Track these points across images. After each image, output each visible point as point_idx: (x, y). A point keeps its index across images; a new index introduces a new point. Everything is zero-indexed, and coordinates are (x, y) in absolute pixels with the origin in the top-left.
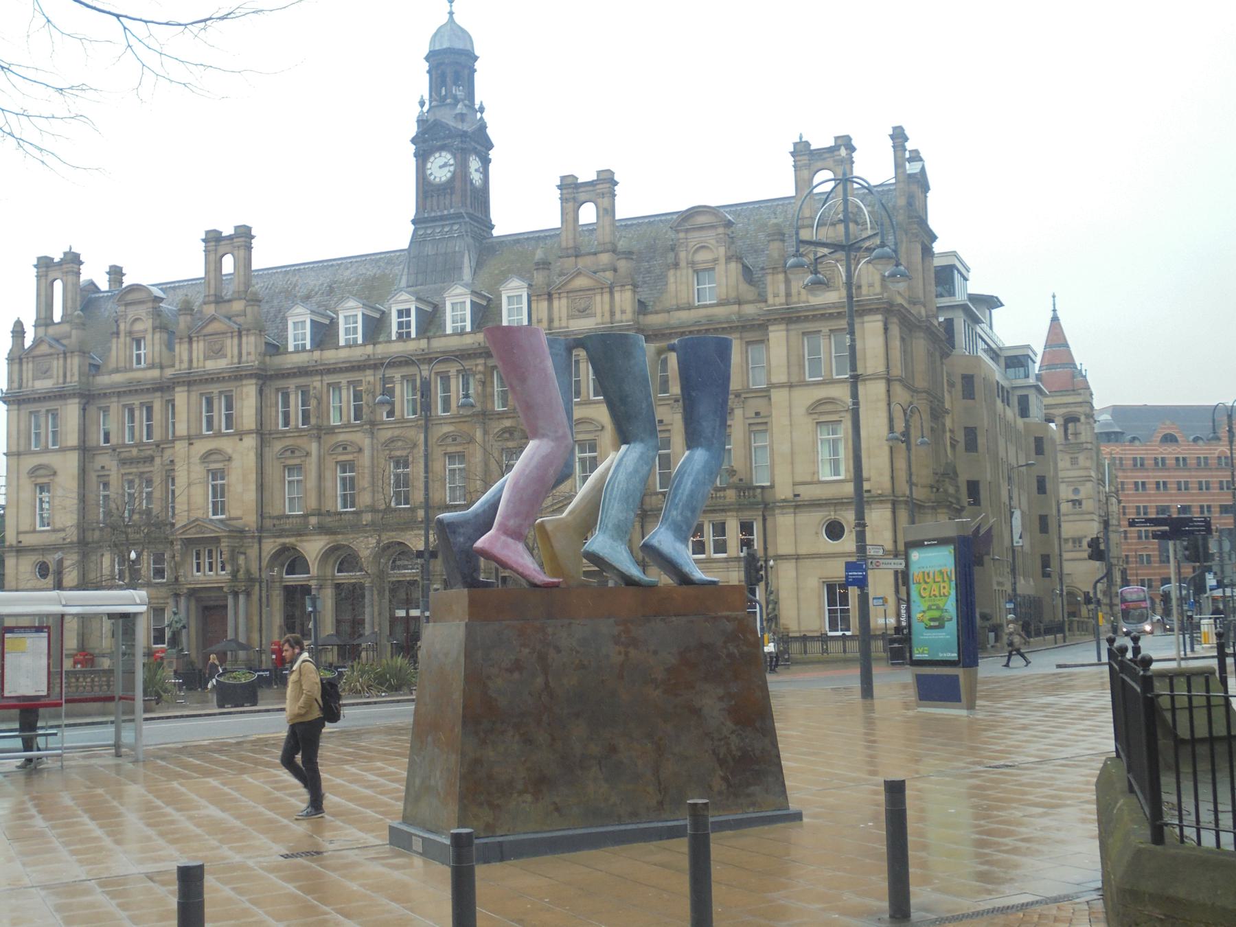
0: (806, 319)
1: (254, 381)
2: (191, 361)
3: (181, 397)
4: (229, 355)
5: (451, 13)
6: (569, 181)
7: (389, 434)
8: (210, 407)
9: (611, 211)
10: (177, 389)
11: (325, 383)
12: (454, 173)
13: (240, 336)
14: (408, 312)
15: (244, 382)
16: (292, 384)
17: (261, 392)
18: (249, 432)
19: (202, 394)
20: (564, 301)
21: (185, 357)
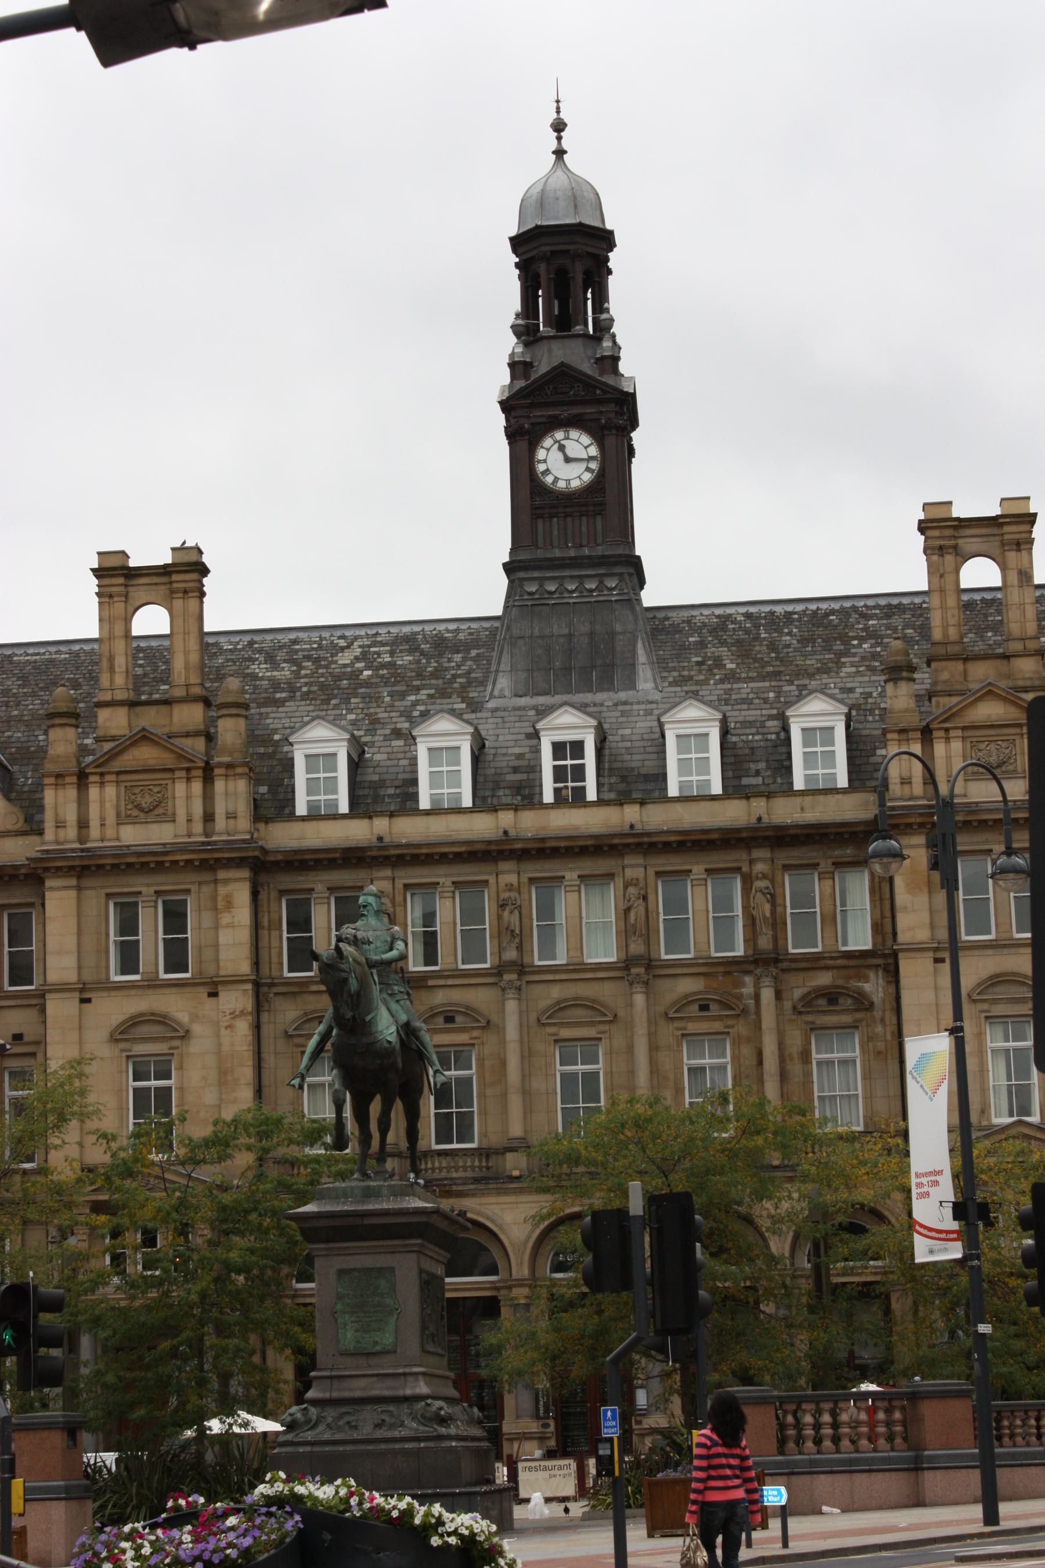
1: (245, 873)
2: (83, 824)
3: (60, 903)
5: (560, 153)
6: (940, 513)
7: (556, 993)
8: (128, 925)
9: (1025, 575)
10: (48, 883)
11: (399, 884)
12: (601, 475)
13: (208, 778)
14: (578, 748)
15: (222, 875)
16: (319, 882)
17: (255, 894)
18: (235, 981)
19: (109, 896)
20: (956, 746)
21: (71, 815)
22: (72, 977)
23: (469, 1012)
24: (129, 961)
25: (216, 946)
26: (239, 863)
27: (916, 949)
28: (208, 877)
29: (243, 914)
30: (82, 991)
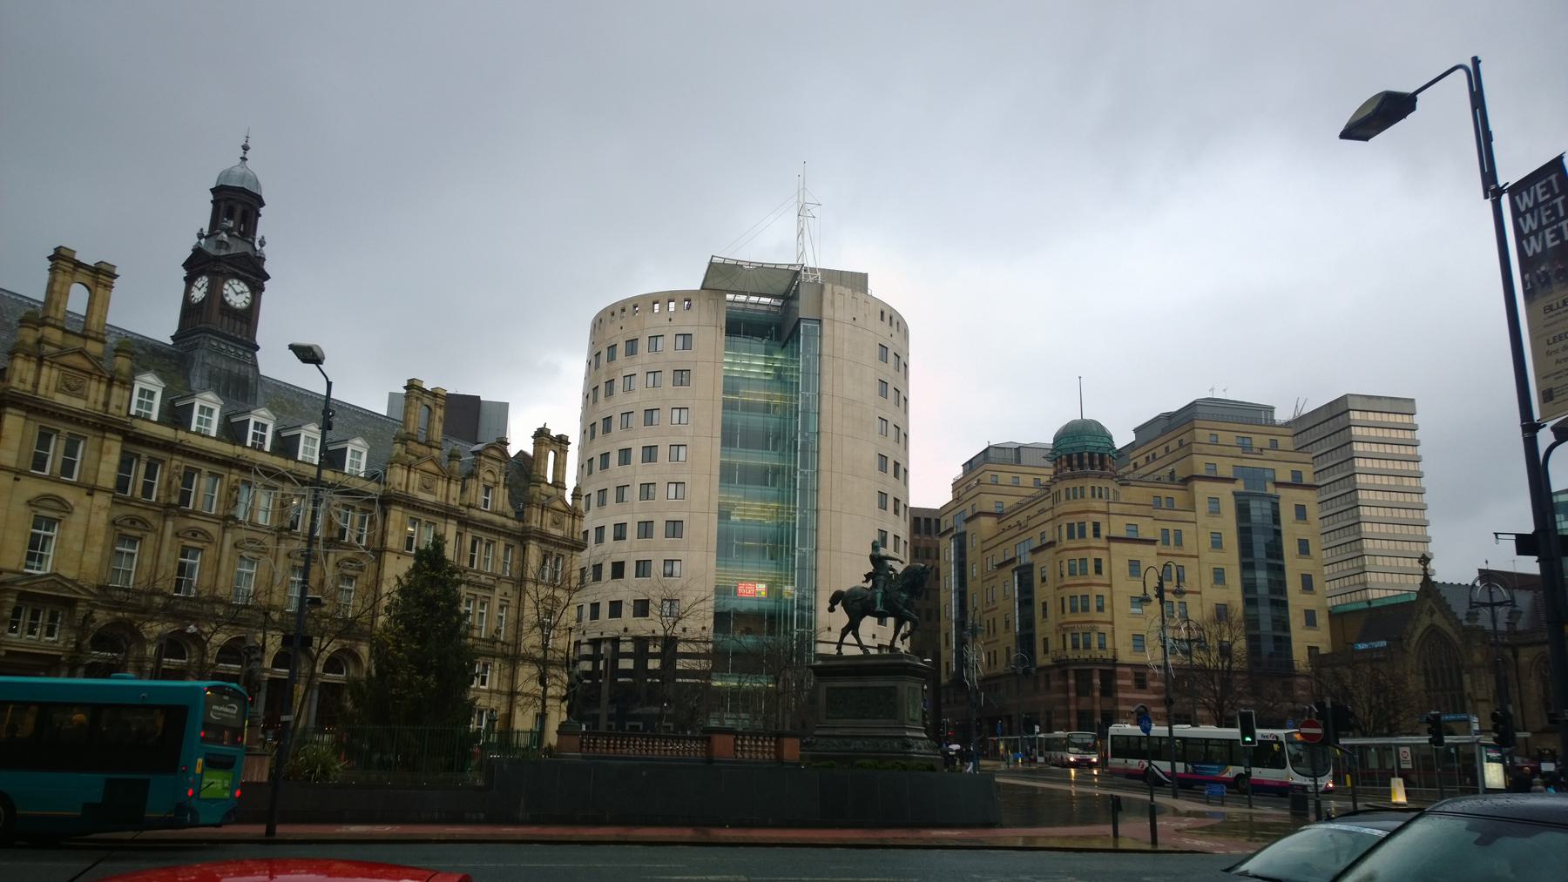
0: (551, 543)
4: (92, 396)
21: (30, 377)
22: (12, 464)
23: (205, 533)
24: (39, 462)
25: (97, 471)
26: (118, 432)
27: (392, 551)
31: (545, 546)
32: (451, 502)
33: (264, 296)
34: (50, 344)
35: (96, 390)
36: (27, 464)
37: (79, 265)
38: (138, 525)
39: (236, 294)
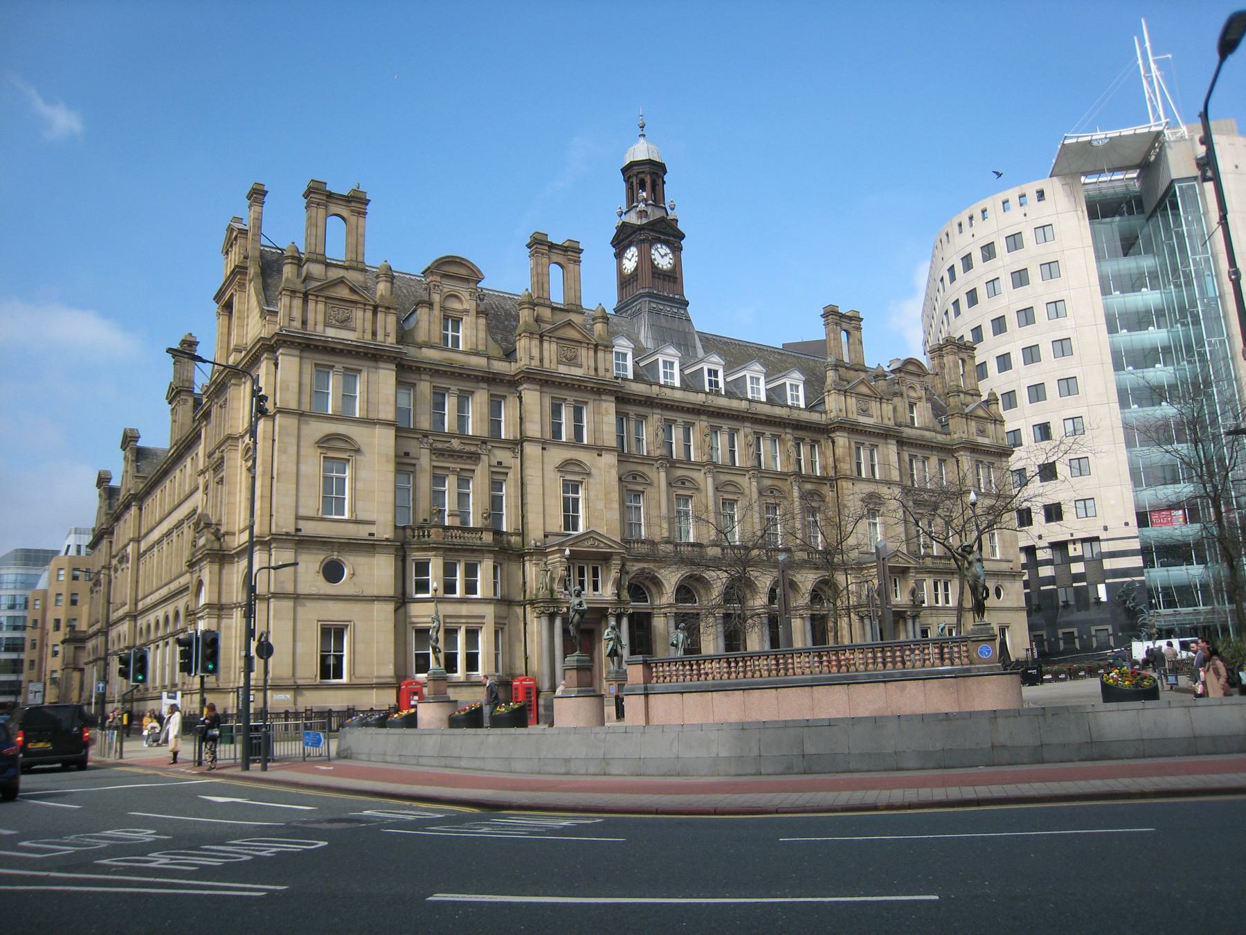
2: (541, 360)
4: (585, 364)
15: (603, 397)
18: (609, 449)
23: (691, 480)
24: (557, 432)
26: (610, 393)
28: (597, 397)
29: (612, 418)
30: (543, 443)
31: (977, 456)
32: (886, 421)
33: (684, 255)
34: (546, 322)
35: (585, 355)
36: (548, 436)
37: (552, 246)
38: (639, 479)
39: (662, 258)
